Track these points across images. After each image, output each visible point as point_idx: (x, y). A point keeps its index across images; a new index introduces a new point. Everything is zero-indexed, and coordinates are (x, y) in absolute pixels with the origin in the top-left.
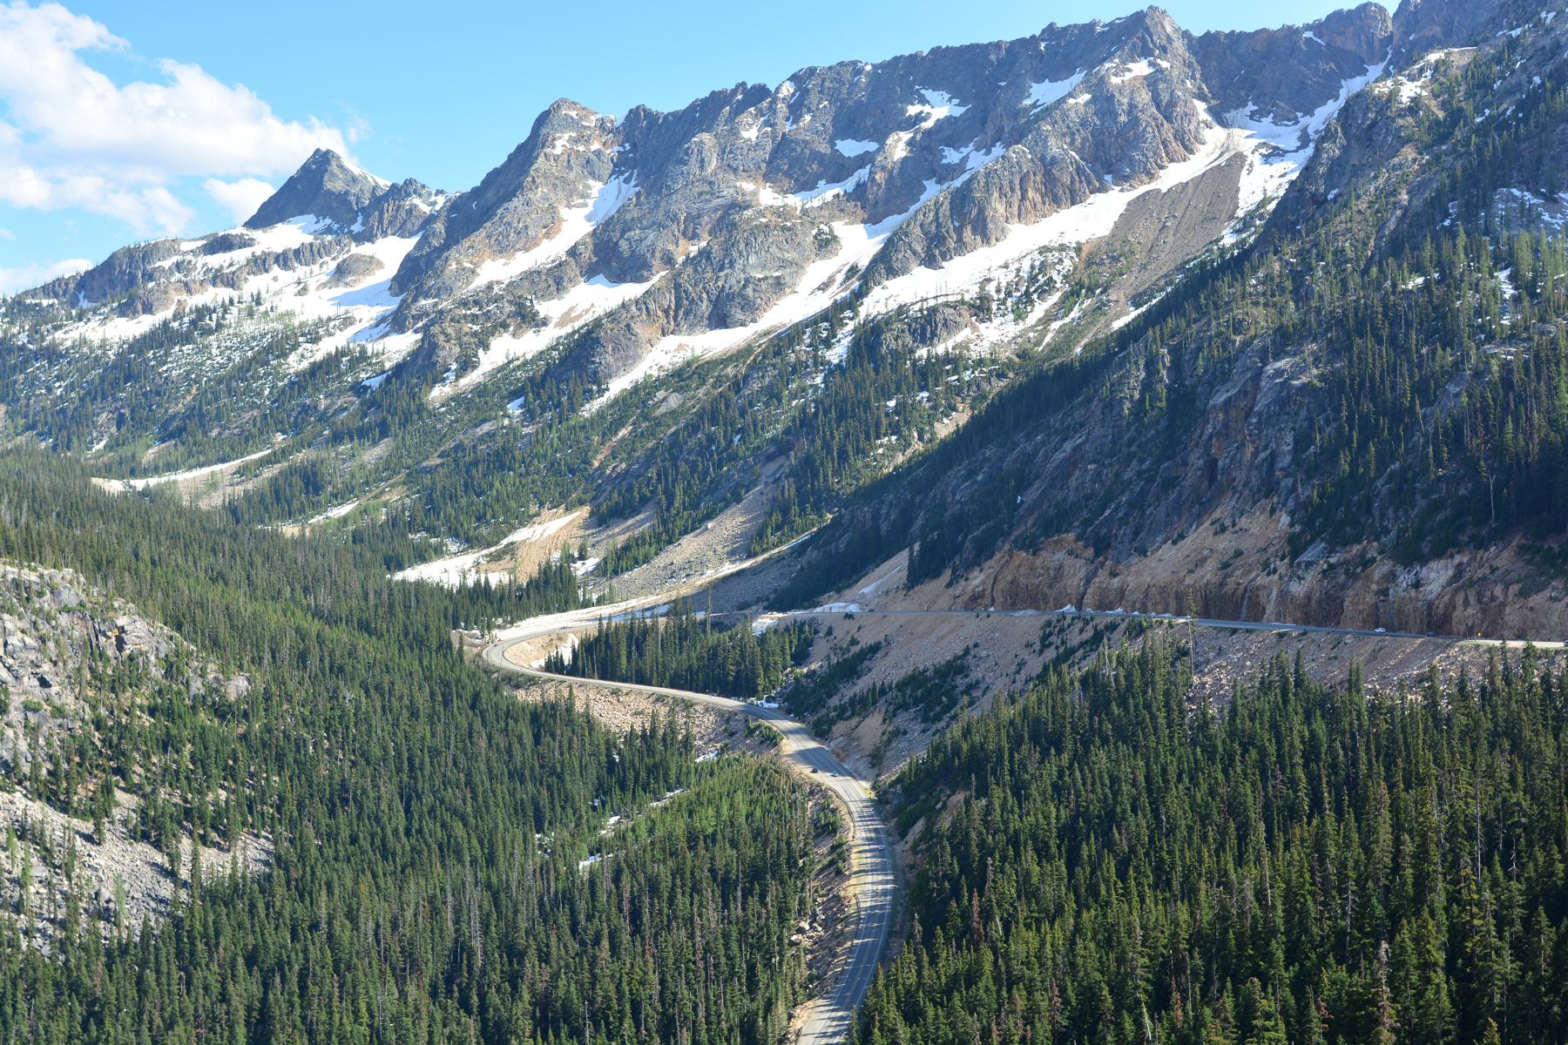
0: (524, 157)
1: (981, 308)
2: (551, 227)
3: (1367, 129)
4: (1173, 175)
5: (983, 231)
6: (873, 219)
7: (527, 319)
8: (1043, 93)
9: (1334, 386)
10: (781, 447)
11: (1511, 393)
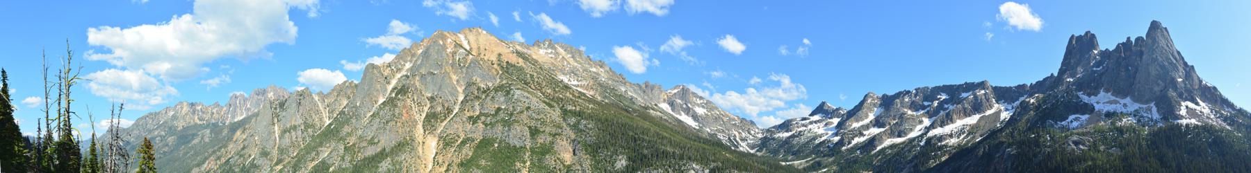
0: (862, 103)
1: (951, 136)
2: (867, 117)
3: (1024, 107)
4: (989, 112)
5: (952, 121)
6: (930, 117)
7: (862, 135)
8: (964, 95)
9: (1019, 154)
10: (911, 161)
11: (1049, 157)
